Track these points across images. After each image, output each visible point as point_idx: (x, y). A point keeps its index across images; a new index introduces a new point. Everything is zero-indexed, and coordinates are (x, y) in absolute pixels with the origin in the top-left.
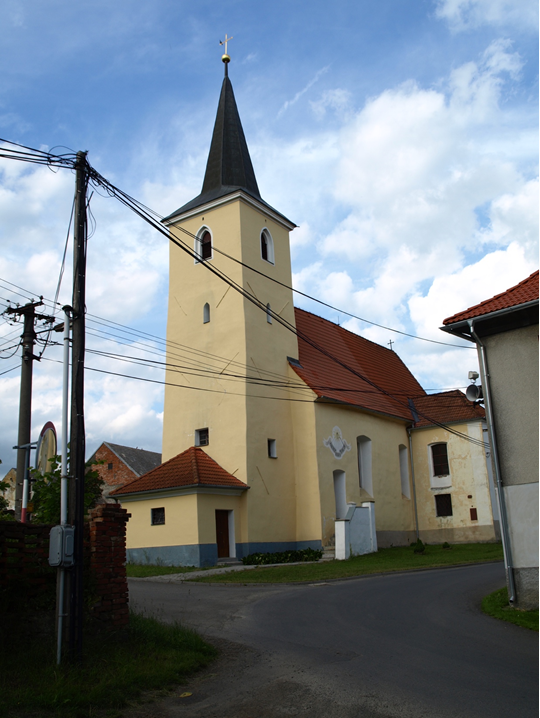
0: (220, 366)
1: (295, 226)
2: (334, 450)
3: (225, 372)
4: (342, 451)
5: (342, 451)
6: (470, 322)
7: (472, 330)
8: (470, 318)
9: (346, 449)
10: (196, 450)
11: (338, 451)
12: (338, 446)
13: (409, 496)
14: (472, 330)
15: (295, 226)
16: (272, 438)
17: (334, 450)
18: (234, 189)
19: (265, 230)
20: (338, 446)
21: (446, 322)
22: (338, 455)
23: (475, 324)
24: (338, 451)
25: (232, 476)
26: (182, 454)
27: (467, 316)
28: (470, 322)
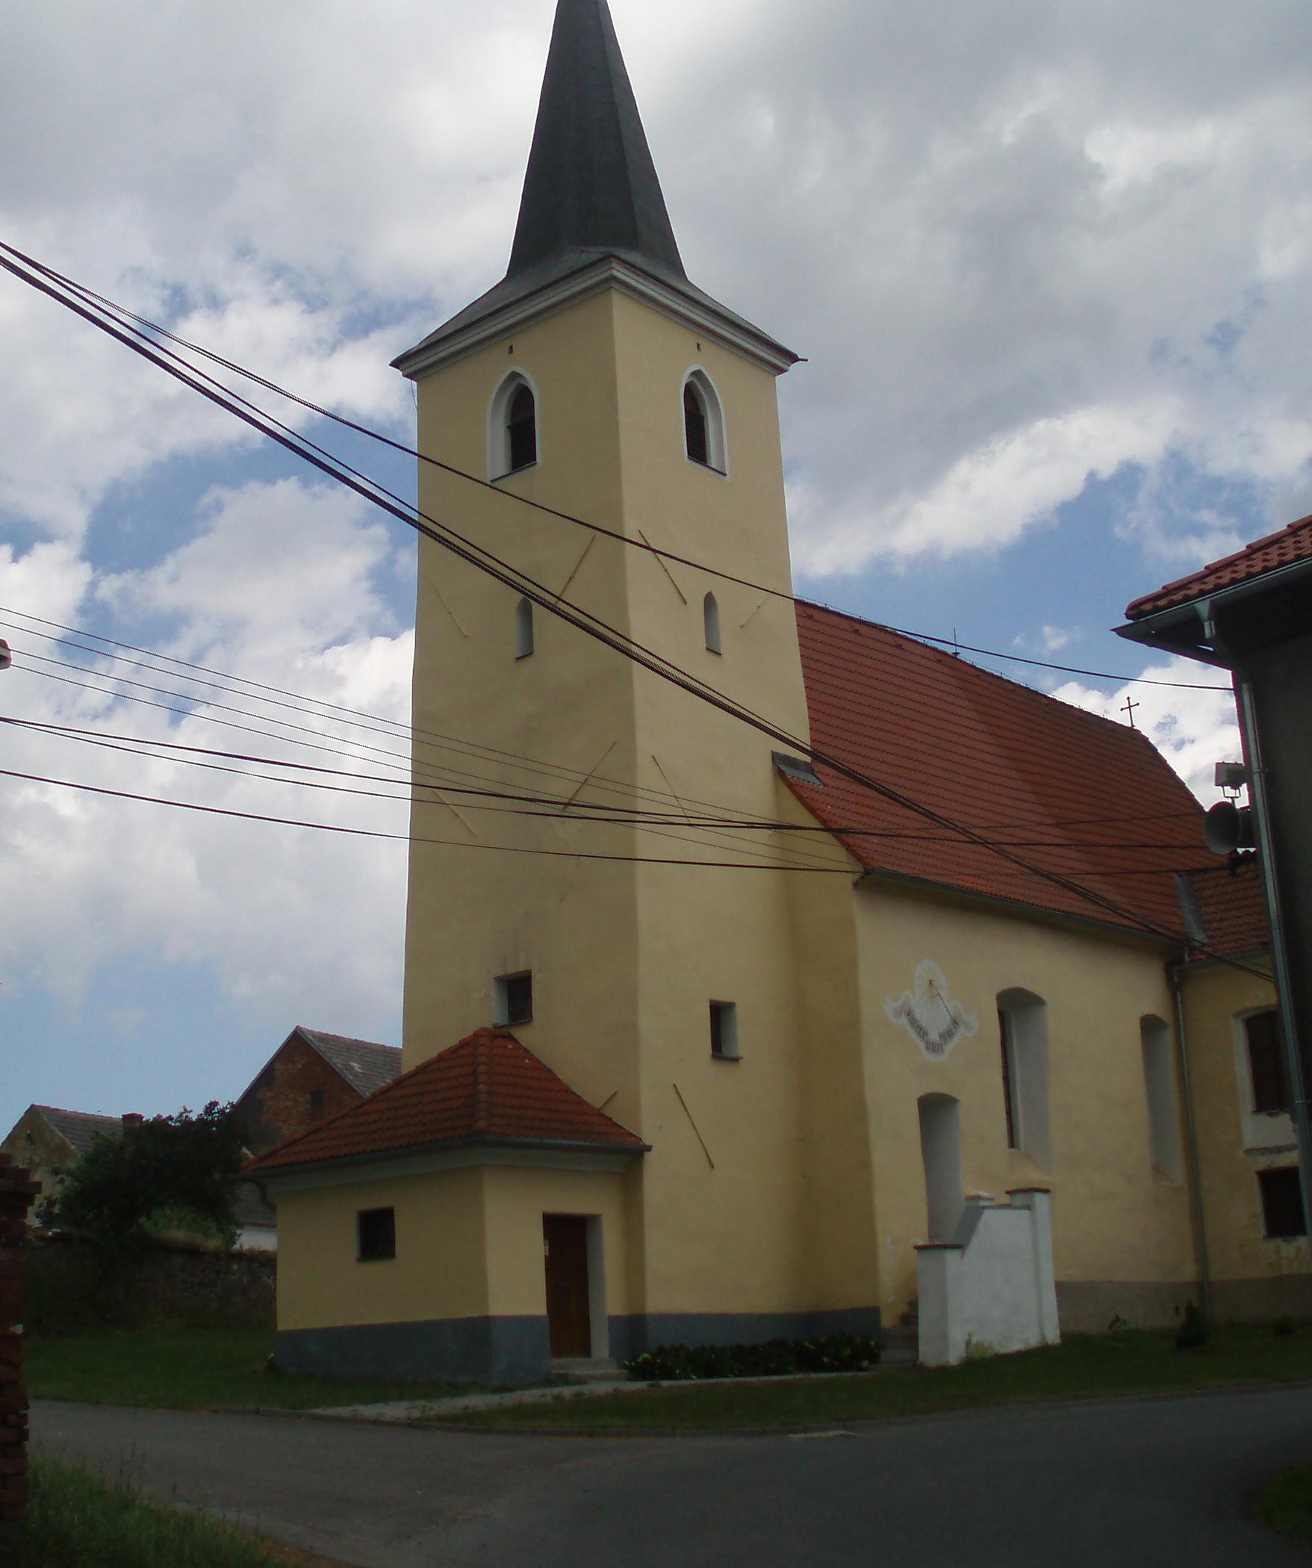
0: (559, 789)
1: (794, 359)
2: (922, 1032)
3: (587, 796)
4: (947, 1035)
5: (947, 1035)
6: (1203, 607)
7: (1208, 630)
8: (1202, 593)
9: (962, 1029)
10: (499, 1035)
11: (934, 1037)
12: (935, 1023)
13: (905, 832)
14: (1208, 630)
15: (794, 359)
16: (722, 997)
17: (922, 1032)
18: (594, 257)
19: (697, 374)
20: (935, 1023)
21: (1135, 611)
22: (933, 1048)
23: (1219, 612)
24: (934, 1037)
25: (599, 1114)
26: (453, 1051)
27: (1195, 589)
28: (1203, 607)
